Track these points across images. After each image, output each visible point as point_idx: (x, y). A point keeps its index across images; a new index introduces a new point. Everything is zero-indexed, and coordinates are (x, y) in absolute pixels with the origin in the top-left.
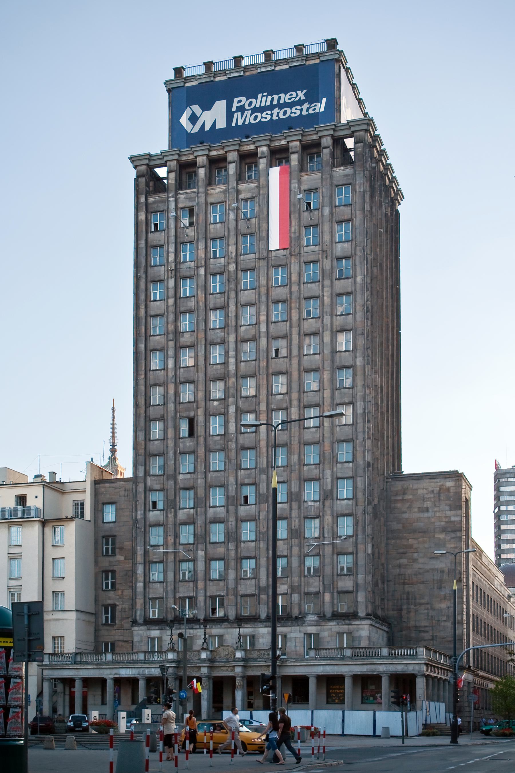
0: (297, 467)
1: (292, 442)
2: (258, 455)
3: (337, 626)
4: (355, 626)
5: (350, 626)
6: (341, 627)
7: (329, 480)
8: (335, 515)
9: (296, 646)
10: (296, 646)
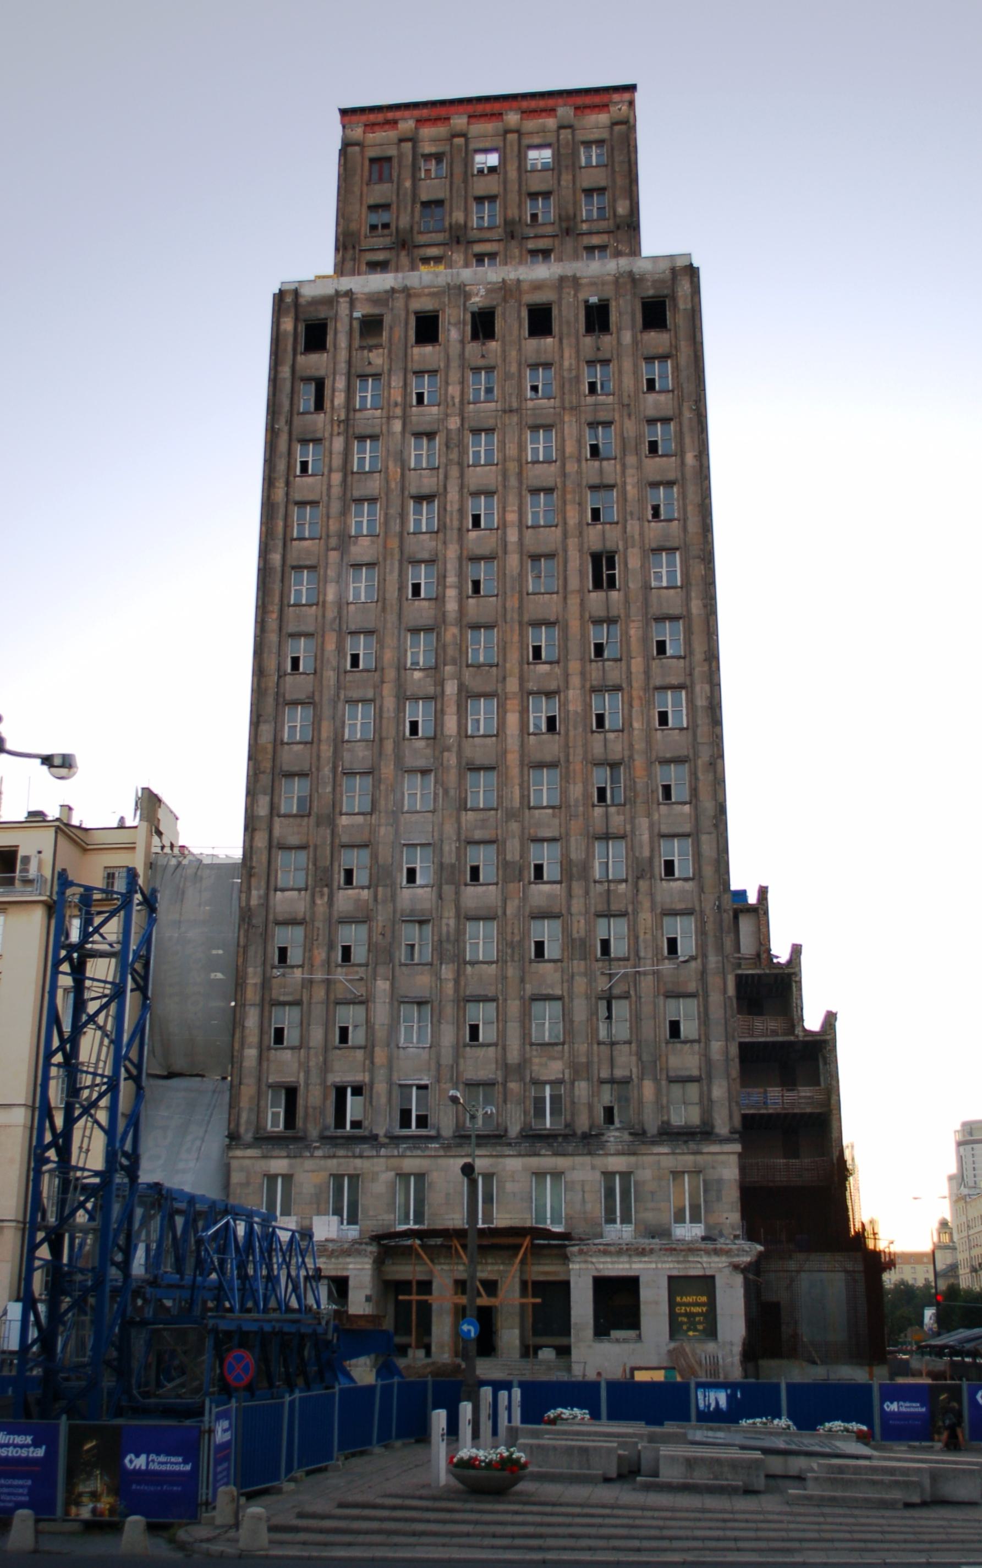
0: (581, 809)
1: (571, 758)
2: (503, 783)
3: (670, 1157)
4: (709, 1158)
5: (699, 1158)
6: (680, 1157)
7: (646, 837)
8: (659, 911)
9: (584, 1201)
10: (584, 1201)
